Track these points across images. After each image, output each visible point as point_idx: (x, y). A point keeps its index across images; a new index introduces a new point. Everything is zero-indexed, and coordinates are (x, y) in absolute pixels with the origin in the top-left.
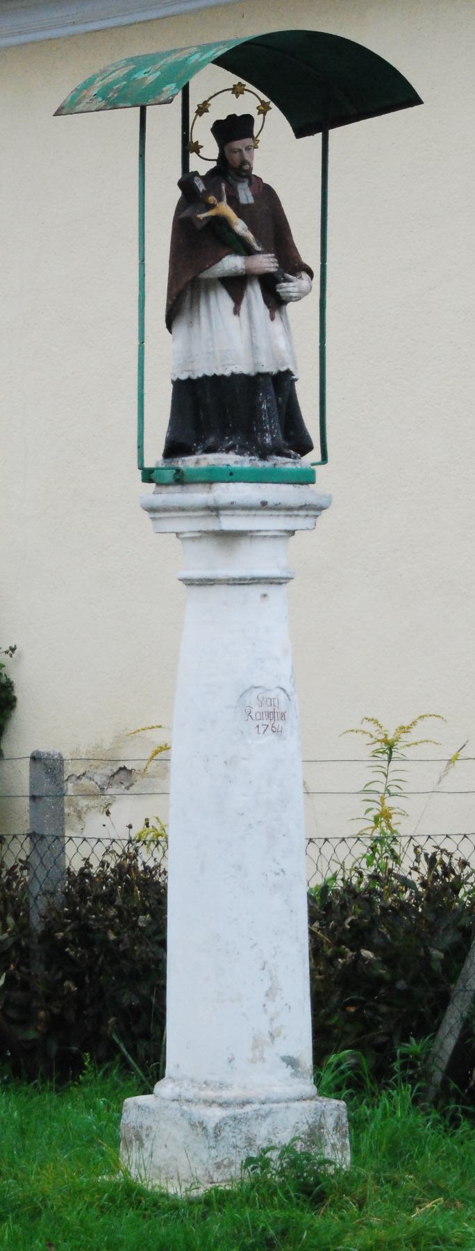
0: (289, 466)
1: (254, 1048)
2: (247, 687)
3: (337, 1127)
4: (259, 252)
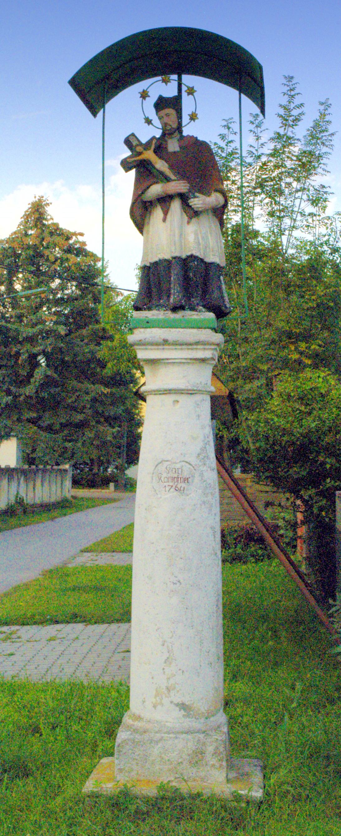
0: (195, 317)
1: (156, 696)
2: (160, 461)
3: (216, 753)
4: (174, 180)
